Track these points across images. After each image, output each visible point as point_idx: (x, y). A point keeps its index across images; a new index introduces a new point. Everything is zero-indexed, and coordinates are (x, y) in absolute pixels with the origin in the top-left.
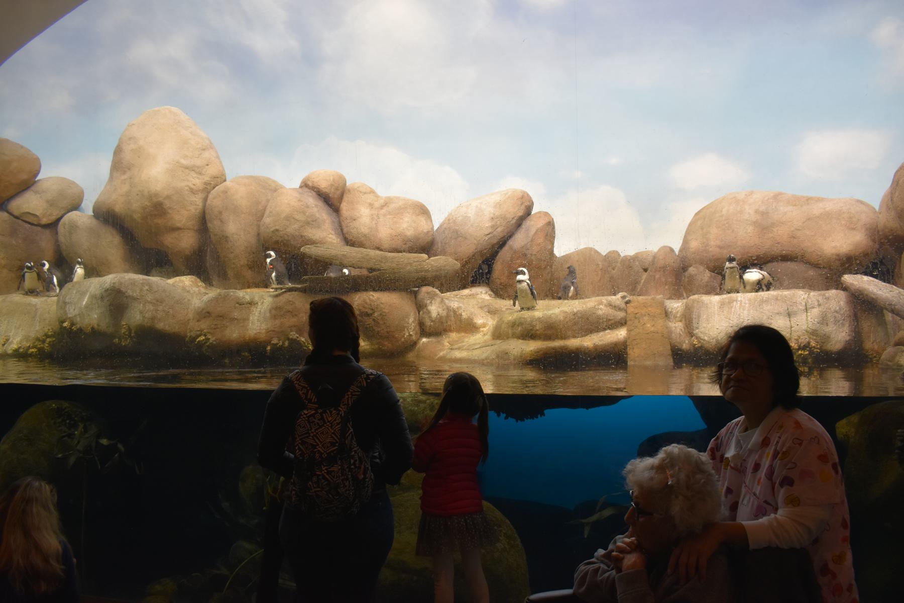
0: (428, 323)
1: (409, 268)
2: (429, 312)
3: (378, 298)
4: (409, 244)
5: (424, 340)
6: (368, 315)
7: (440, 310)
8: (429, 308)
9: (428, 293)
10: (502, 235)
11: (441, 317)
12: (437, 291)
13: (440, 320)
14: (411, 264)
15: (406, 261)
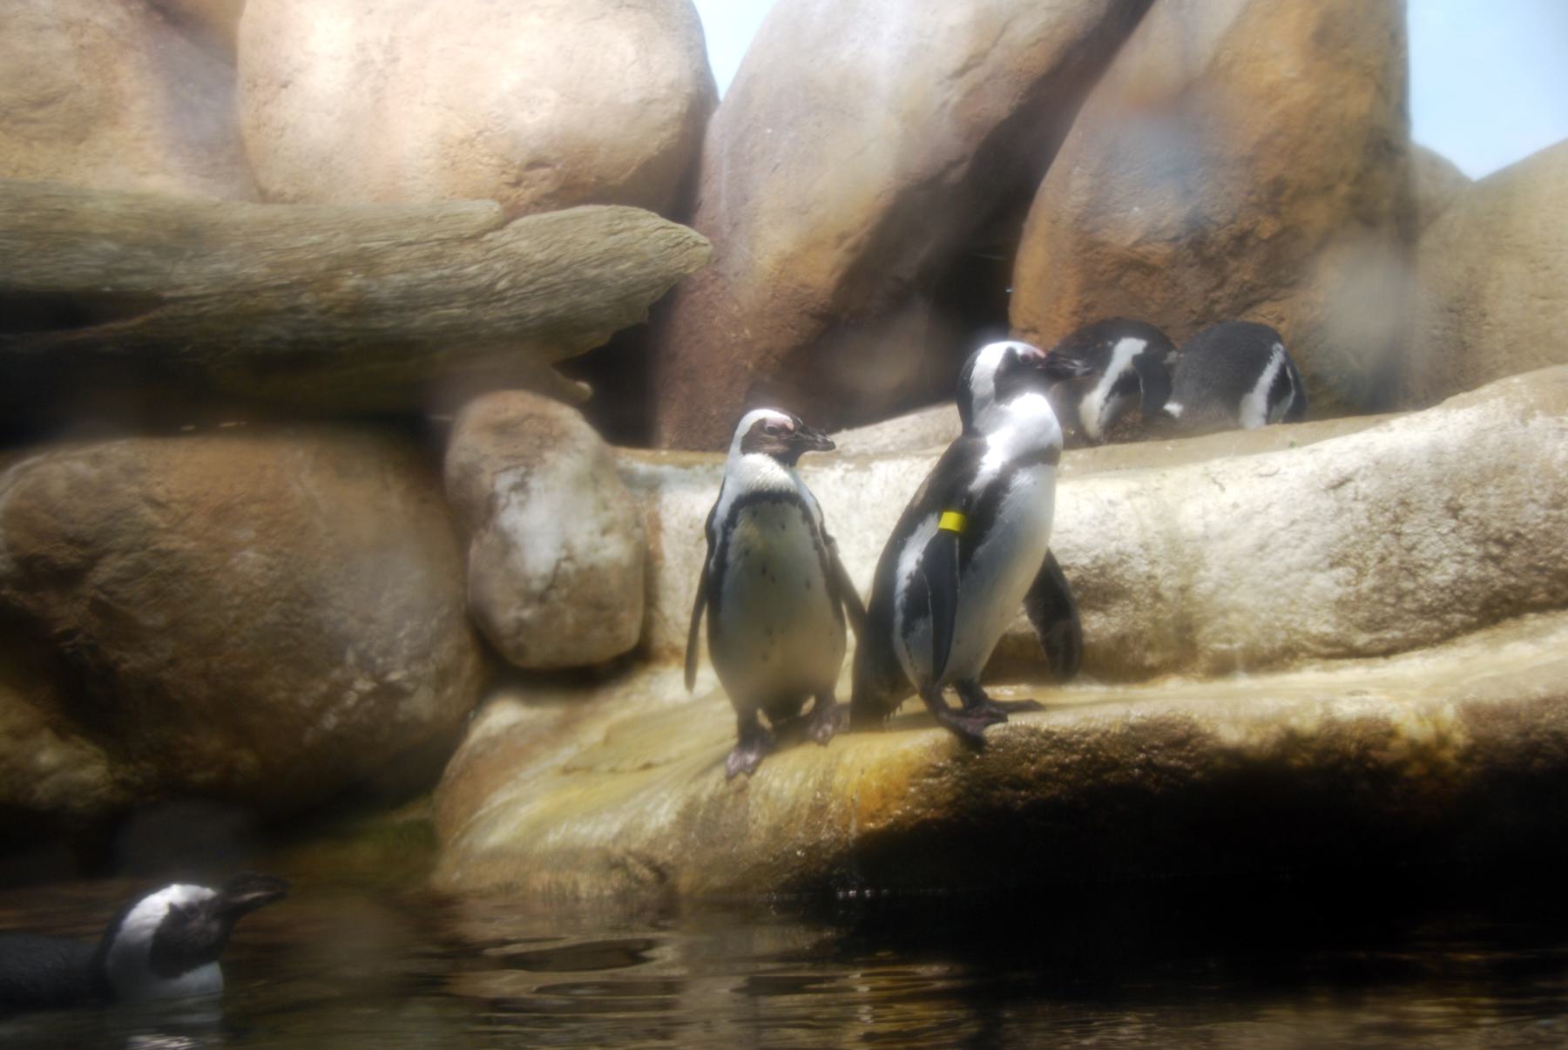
0: (509, 614)
1: (351, 281)
2: (507, 545)
3: (130, 472)
4: (542, 181)
5: (504, 715)
6: (67, 578)
7: (583, 534)
8: (509, 518)
9: (503, 430)
10: (1040, 61)
11: (590, 574)
12: (570, 419)
13: (575, 586)
14: (366, 261)
15: (341, 244)
